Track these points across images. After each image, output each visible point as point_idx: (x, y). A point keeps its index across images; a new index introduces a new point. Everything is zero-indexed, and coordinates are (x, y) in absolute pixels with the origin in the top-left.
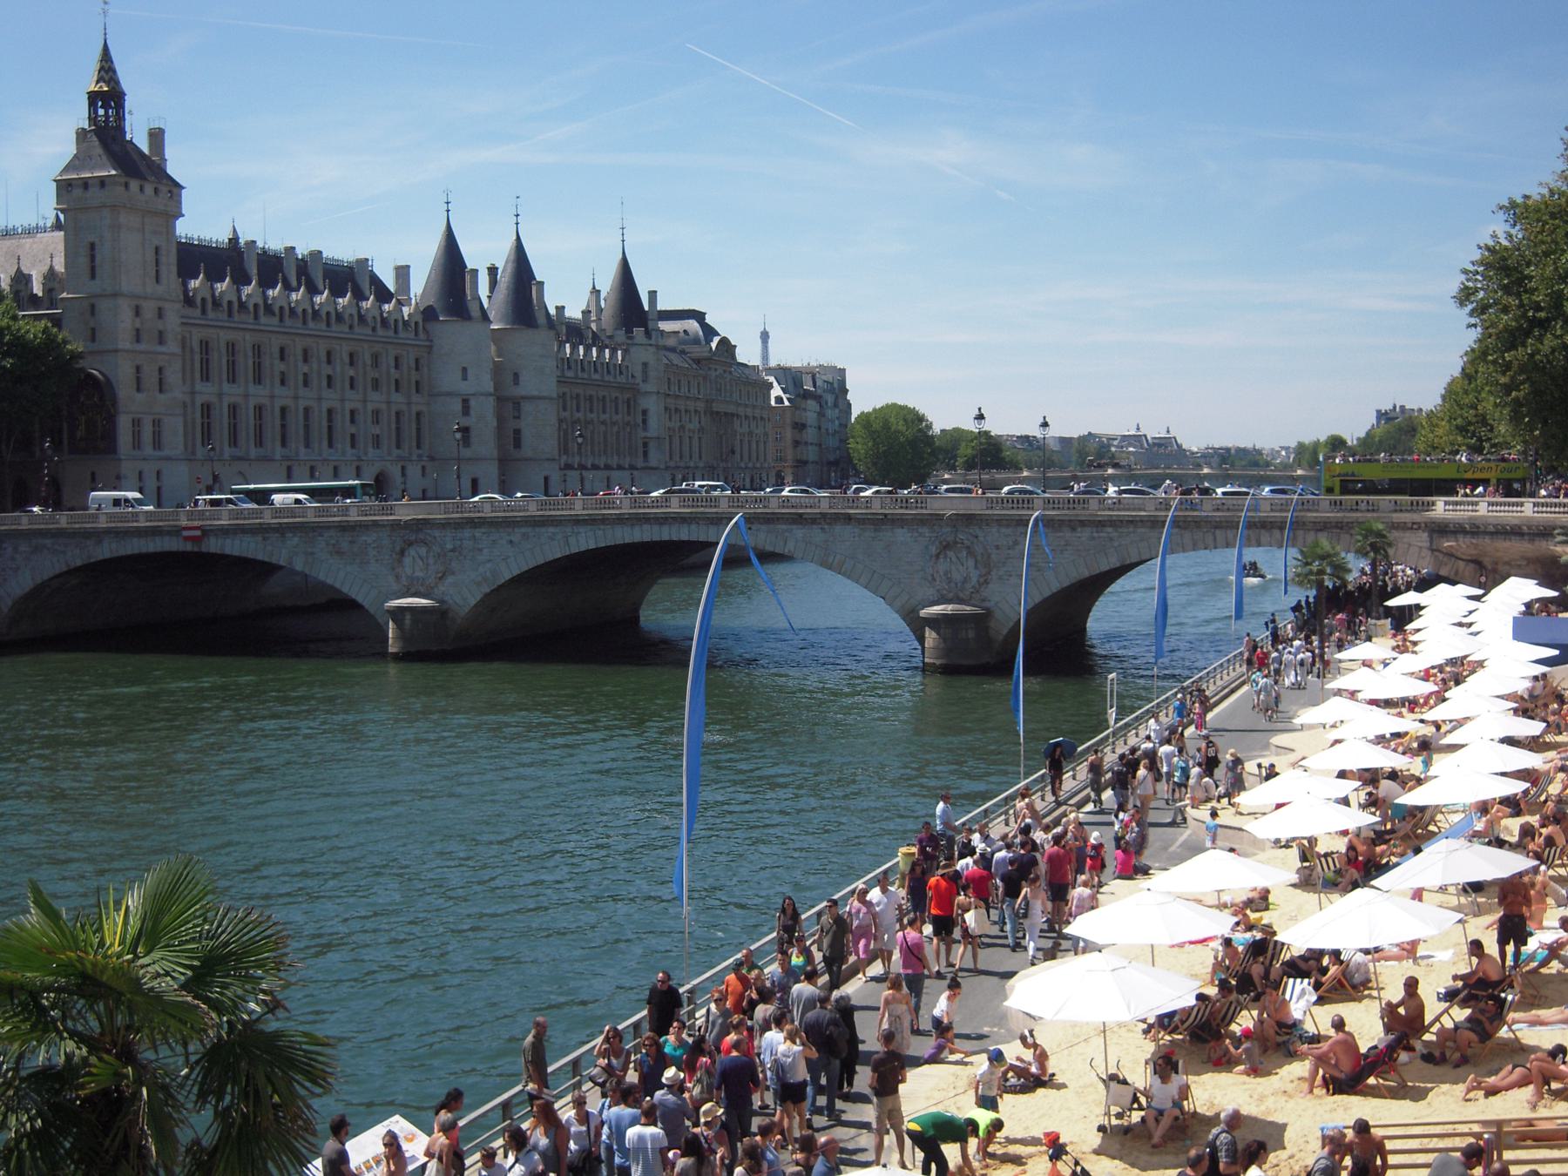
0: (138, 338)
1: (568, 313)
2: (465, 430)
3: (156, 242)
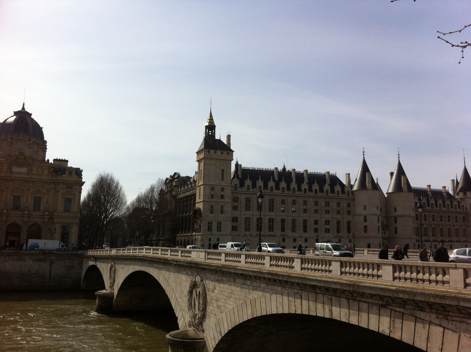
0: (212, 196)
1: (432, 187)
2: (366, 227)
3: (222, 168)
